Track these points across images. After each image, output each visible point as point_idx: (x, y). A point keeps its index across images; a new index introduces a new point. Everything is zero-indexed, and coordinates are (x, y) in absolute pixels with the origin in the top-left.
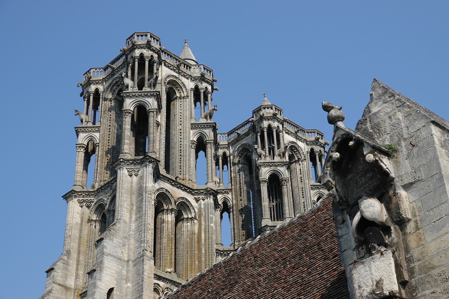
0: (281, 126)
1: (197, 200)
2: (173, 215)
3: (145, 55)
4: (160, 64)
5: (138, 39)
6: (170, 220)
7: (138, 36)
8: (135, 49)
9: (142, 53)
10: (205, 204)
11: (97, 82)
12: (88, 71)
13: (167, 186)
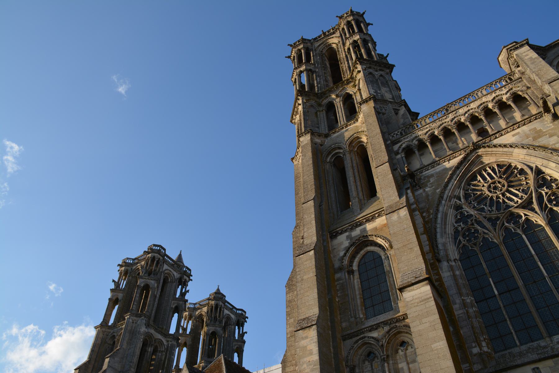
0: (223, 305)
1: (168, 341)
2: (152, 348)
4: (164, 263)
6: (149, 350)
10: (171, 344)
13: (152, 331)
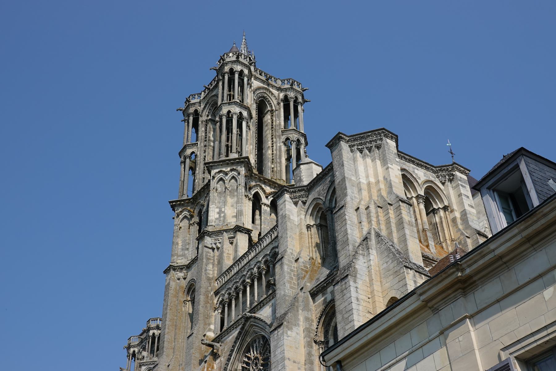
3: (156, 334)
5: (152, 323)
7: (152, 321)
8: (150, 330)
9: (154, 333)
11: (134, 346)
12: (130, 338)
